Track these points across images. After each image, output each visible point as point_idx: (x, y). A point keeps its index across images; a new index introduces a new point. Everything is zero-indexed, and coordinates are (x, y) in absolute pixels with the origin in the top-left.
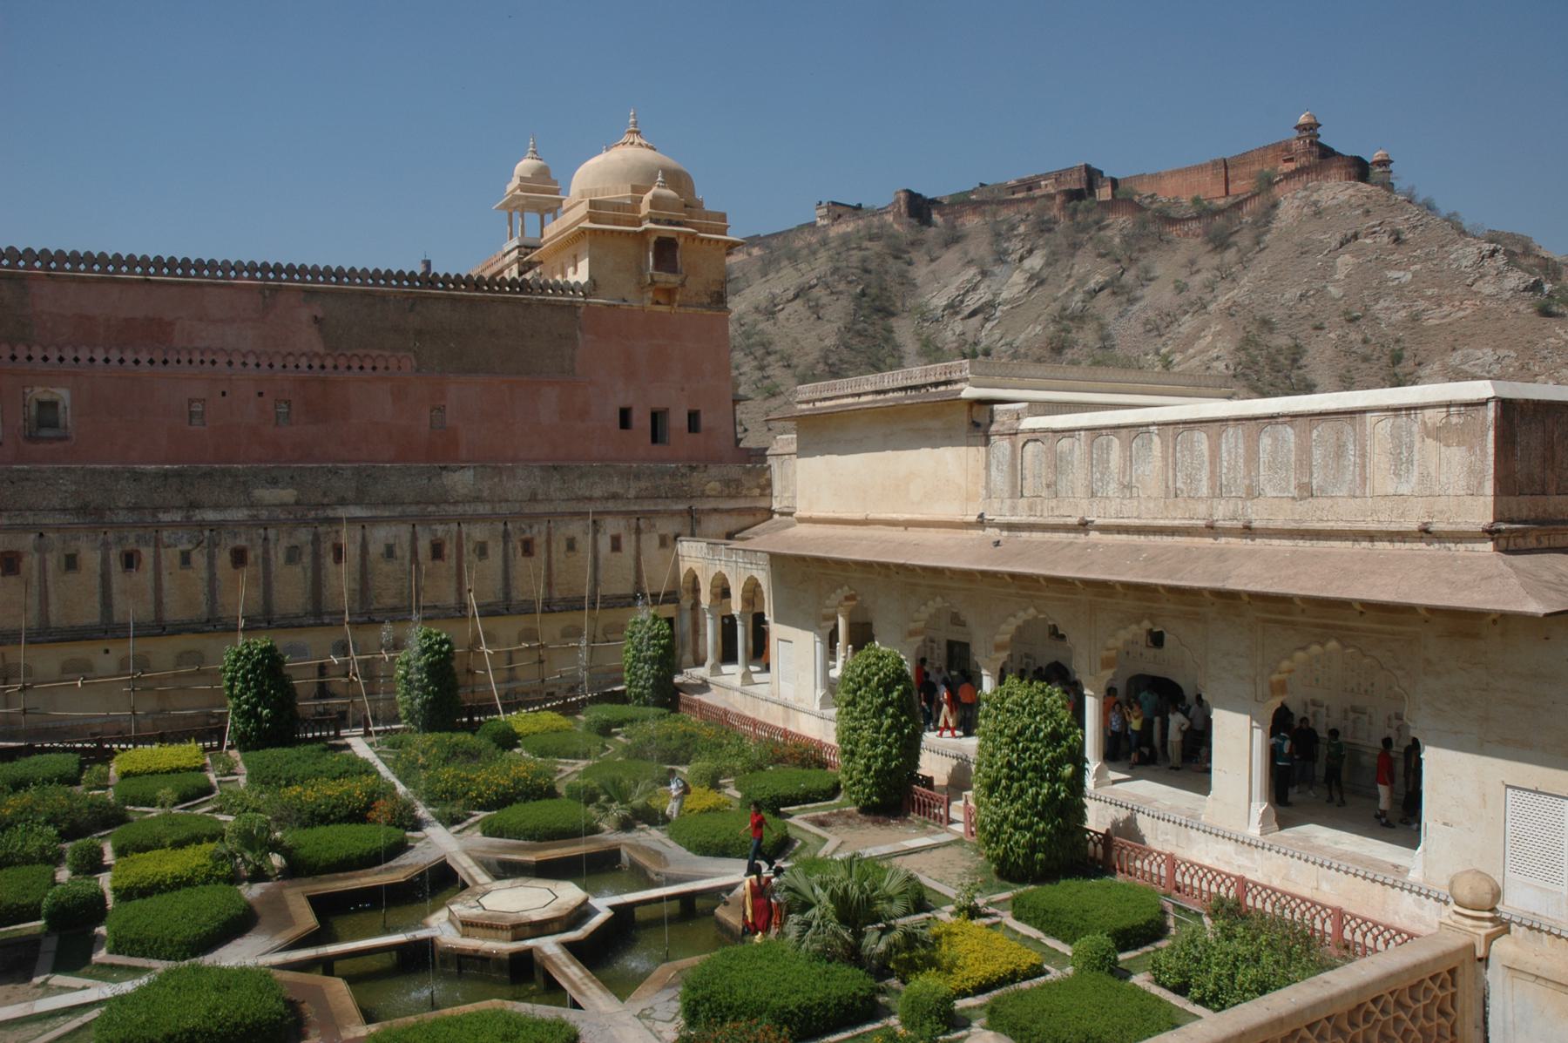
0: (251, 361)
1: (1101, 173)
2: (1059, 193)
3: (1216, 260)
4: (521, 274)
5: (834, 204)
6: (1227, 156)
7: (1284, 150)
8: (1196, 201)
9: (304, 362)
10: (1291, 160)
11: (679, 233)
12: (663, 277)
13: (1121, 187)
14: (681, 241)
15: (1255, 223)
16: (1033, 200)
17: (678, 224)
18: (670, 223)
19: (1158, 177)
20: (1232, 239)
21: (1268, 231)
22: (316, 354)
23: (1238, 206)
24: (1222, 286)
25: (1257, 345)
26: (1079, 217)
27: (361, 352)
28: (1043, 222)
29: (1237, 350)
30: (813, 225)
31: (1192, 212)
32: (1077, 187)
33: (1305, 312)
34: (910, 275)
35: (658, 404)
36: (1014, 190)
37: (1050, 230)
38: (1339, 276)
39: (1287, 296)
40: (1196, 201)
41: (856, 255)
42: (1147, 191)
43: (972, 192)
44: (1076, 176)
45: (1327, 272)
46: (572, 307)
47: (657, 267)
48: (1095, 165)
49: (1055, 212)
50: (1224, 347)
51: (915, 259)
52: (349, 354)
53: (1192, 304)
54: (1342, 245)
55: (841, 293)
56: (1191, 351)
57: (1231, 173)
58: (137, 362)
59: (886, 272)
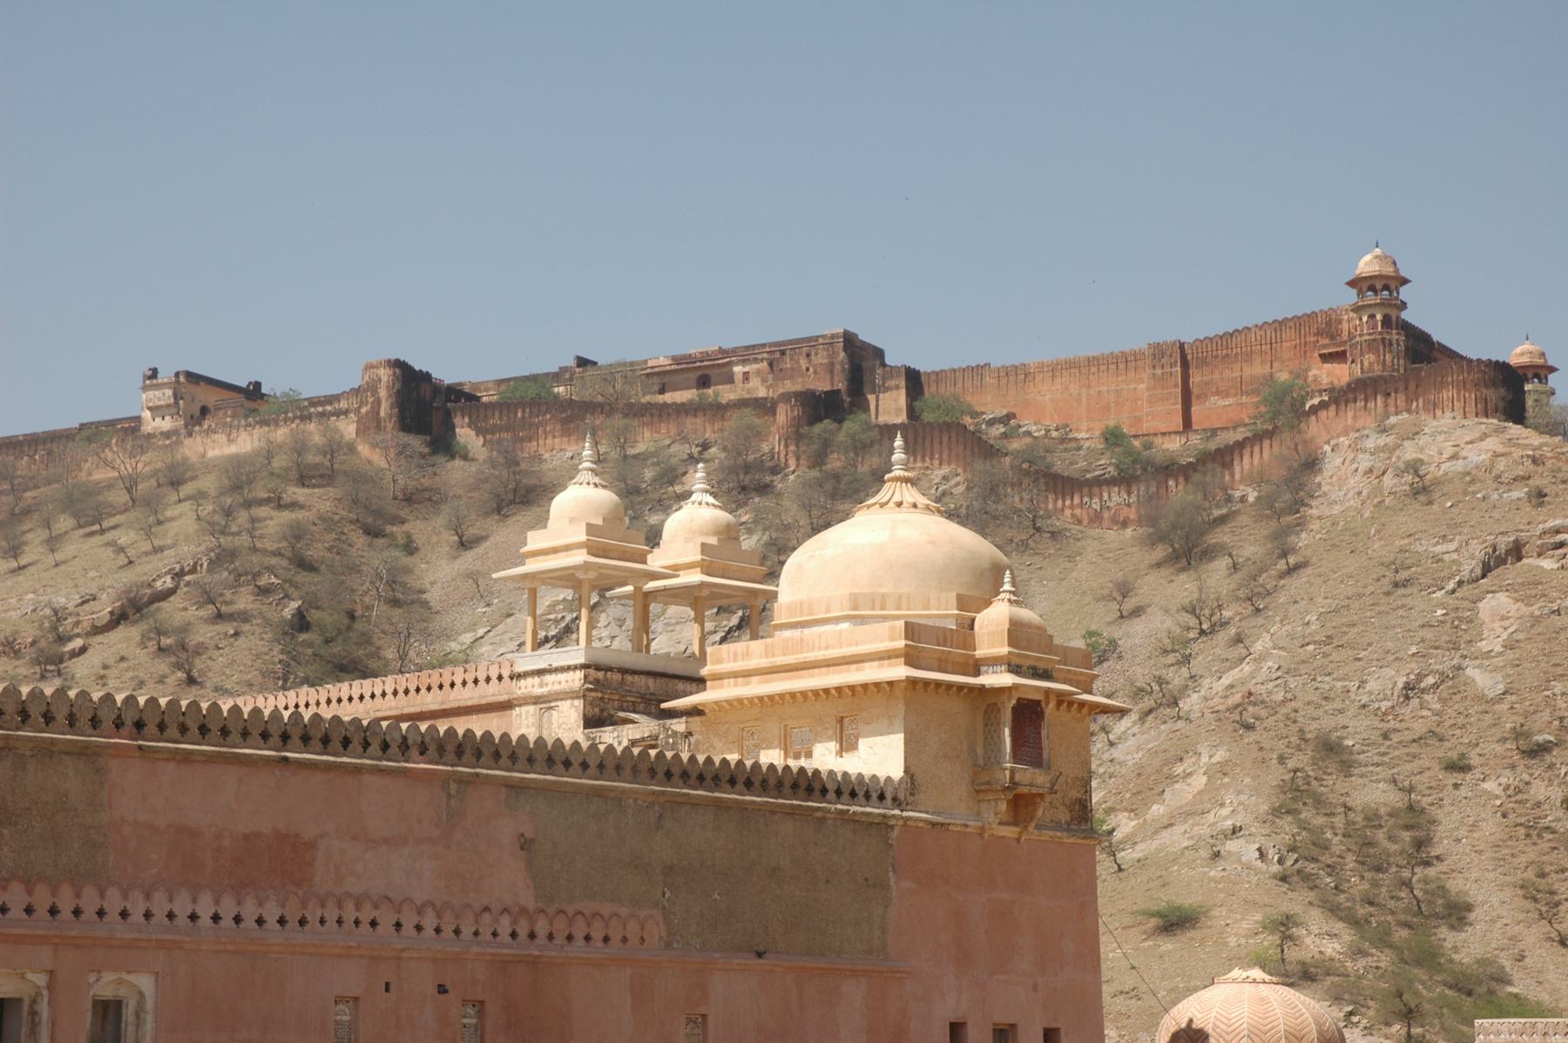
0: (429, 922)
1: (879, 353)
2: (786, 397)
3: (1184, 587)
4: (591, 722)
5: (194, 378)
6: (1188, 338)
7: (1322, 333)
8: (1113, 438)
9: (505, 926)
10: (1339, 357)
11: (1048, 691)
12: (1030, 776)
13: (929, 391)
14: (1050, 709)
15: (1266, 502)
16: (718, 410)
17: (1046, 675)
18: (1036, 673)
19: (1019, 374)
20: (1221, 536)
21: (1301, 524)
22: (524, 910)
23: (1224, 457)
24: (1206, 653)
25: (1319, 802)
26: (835, 462)
27: (588, 907)
28: (747, 468)
29: (1276, 812)
30: (129, 429)
31: (1106, 465)
32: (822, 386)
33: (1419, 728)
34: (411, 580)
35: (1003, 1018)
36: (664, 380)
37: (764, 489)
38: (1492, 642)
39: (1372, 685)
40: (1113, 438)
41: (275, 522)
42: (992, 407)
43: (557, 377)
44: (821, 358)
45: (1459, 632)
46: (883, 824)
47: (1016, 757)
48: (866, 336)
49: (773, 443)
50: (1243, 803)
51: (419, 540)
52: (570, 910)
53: (1138, 693)
54: (1486, 570)
55: (244, 617)
56: (1157, 810)
57: (1196, 378)
58: (260, 921)
59: (355, 569)
